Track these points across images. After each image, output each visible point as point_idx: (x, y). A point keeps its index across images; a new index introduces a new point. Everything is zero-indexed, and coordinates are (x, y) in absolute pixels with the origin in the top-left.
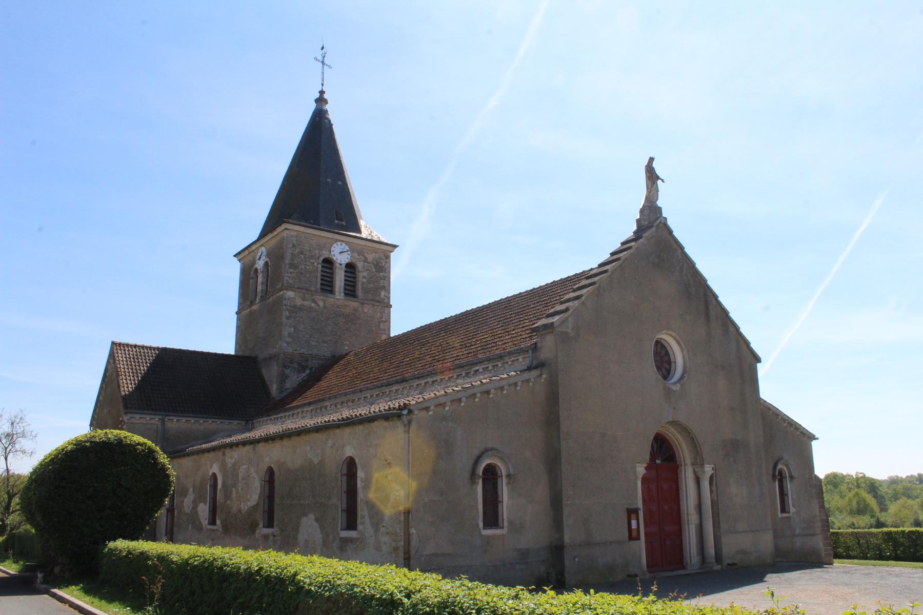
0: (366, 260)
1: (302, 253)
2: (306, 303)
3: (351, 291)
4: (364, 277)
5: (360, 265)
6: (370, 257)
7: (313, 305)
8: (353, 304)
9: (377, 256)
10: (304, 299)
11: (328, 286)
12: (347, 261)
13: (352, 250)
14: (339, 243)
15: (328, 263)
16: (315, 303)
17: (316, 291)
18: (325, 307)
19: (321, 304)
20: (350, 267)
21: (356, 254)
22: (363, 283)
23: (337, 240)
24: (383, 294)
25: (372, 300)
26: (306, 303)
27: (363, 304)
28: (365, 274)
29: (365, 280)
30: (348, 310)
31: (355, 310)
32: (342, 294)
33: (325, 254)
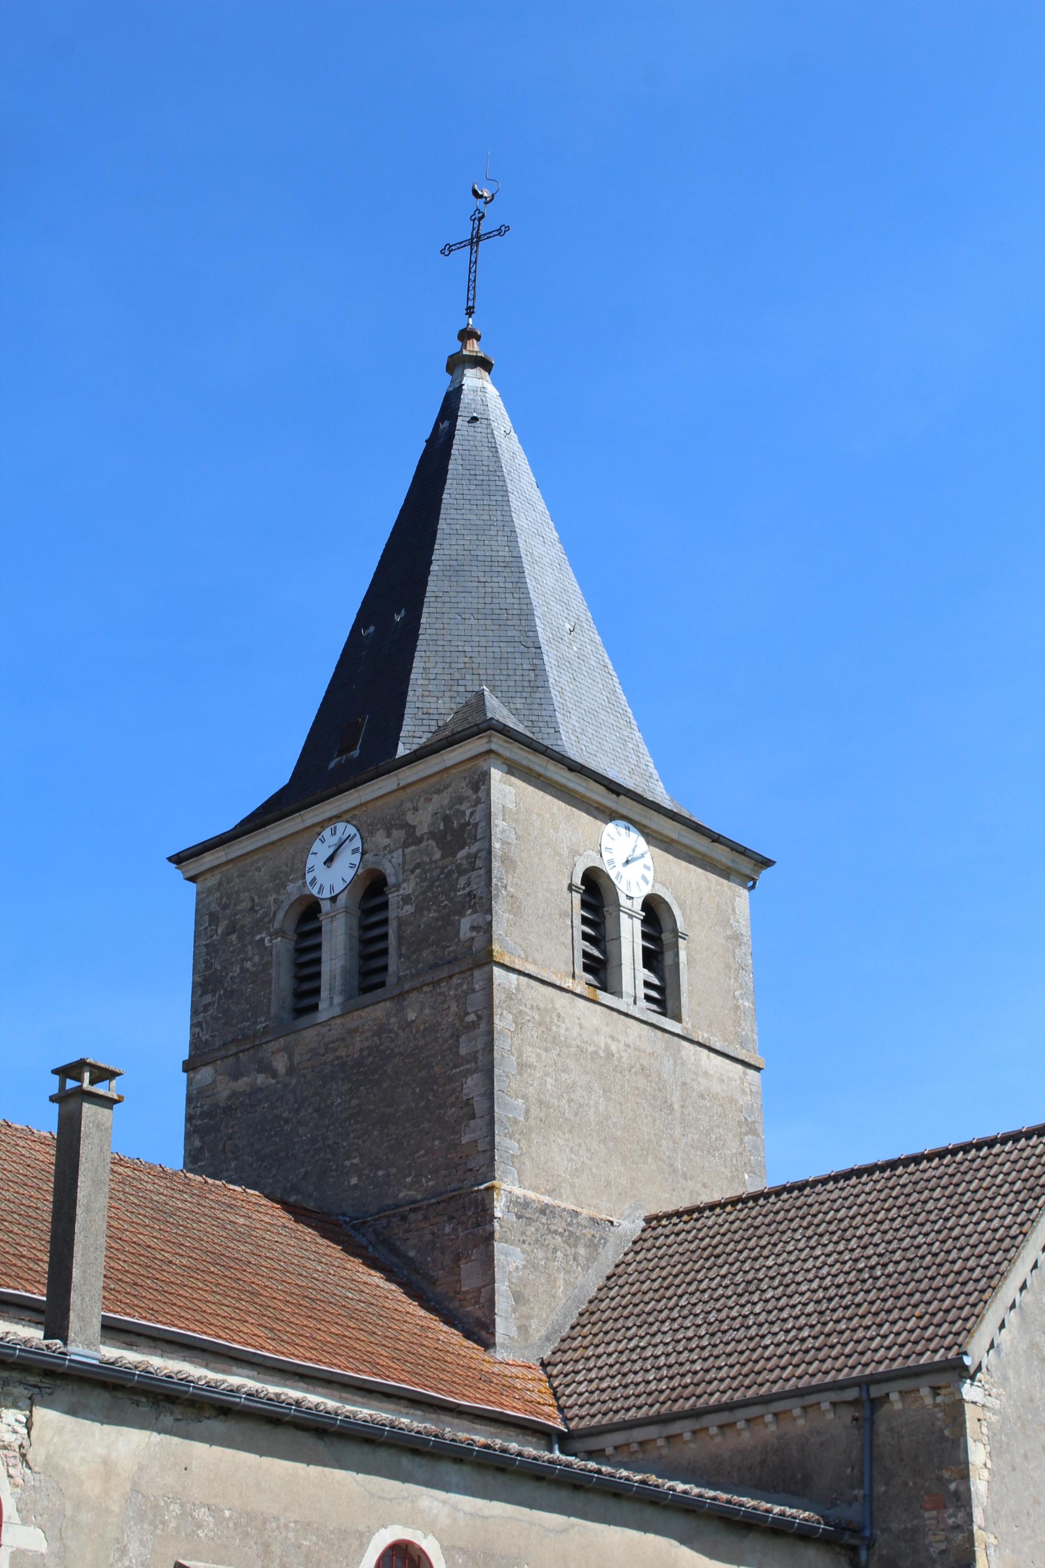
0: (412, 838)
1: (231, 929)
2: (242, 1084)
3: (369, 974)
4: (406, 900)
5: (389, 869)
6: (423, 820)
7: (261, 1079)
8: (378, 1012)
9: (443, 800)
10: (236, 1076)
12: (349, 875)
13: (365, 832)
14: (327, 833)
15: (310, 910)
16: (266, 1068)
17: (266, 1030)
18: (291, 1071)
19: (280, 1064)
20: (372, 889)
21: (381, 839)
22: (401, 923)
23: (322, 825)
24: (465, 924)
25: (434, 967)
26: (242, 1084)
27: (402, 996)
28: (408, 888)
29: (409, 909)
30: (359, 1042)
31: (381, 1030)
32: (338, 1000)
33: (293, 890)
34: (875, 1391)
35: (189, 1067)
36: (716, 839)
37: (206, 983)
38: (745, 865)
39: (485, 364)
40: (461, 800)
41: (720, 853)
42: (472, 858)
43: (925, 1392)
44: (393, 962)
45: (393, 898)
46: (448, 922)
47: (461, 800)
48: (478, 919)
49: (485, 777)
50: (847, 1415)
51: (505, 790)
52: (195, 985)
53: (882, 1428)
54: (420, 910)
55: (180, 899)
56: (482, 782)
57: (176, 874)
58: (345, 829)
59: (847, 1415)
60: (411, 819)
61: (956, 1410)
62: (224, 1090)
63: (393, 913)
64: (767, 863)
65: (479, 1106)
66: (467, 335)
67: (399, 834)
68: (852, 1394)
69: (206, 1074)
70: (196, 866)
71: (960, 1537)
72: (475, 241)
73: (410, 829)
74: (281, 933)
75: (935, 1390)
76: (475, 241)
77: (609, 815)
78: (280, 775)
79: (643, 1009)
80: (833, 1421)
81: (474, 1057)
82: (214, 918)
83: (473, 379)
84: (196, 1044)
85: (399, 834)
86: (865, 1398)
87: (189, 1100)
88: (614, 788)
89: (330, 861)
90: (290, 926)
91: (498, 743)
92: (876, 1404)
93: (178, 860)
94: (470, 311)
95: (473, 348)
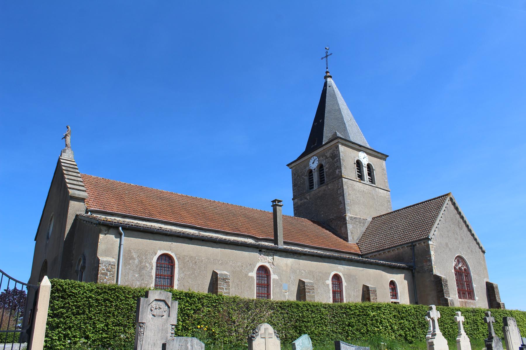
0: (327, 158)
2: (302, 201)
3: (322, 181)
4: (327, 168)
5: (323, 163)
6: (328, 154)
7: (305, 200)
8: (324, 187)
10: (301, 200)
11: (311, 186)
15: (311, 171)
16: (306, 199)
19: (308, 198)
20: (321, 167)
21: (321, 158)
22: (326, 172)
23: (311, 157)
24: (337, 171)
26: (302, 201)
27: (328, 184)
28: (327, 166)
31: (324, 190)
34: (414, 244)
35: (293, 199)
36: (379, 153)
37: (295, 185)
38: (384, 157)
39: (331, 77)
40: (334, 150)
41: (379, 155)
42: (337, 160)
43: (422, 243)
44: (325, 179)
45: (324, 168)
46: (334, 171)
47: (334, 150)
48: (339, 170)
49: (338, 146)
50: (409, 248)
51: (341, 148)
52: (293, 186)
53: (415, 250)
54: (329, 170)
55: (289, 171)
56: (337, 147)
57: (288, 168)
58: (315, 157)
59: (409, 248)
60: (326, 154)
61: (428, 246)
62: (299, 203)
63: (325, 171)
64: (388, 156)
65: (342, 202)
66: (327, 72)
67: (324, 157)
68: (410, 244)
69: (296, 200)
70: (291, 166)
71: (430, 267)
72: (327, 56)
73: (326, 156)
74: (306, 176)
75: (424, 243)
76: (327, 56)
77: (360, 151)
78: (303, 149)
79: (369, 183)
80: (407, 249)
81: (340, 193)
82: (295, 174)
83: (329, 80)
84: (294, 196)
85: (324, 157)
86: (412, 245)
87: (294, 205)
88: (360, 146)
89: (313, 163)
90: (308, 174)
91: (340, 140)
92: (414, 246)
93: (288, 165)
94: (327, 68)
95: (328, 74)
